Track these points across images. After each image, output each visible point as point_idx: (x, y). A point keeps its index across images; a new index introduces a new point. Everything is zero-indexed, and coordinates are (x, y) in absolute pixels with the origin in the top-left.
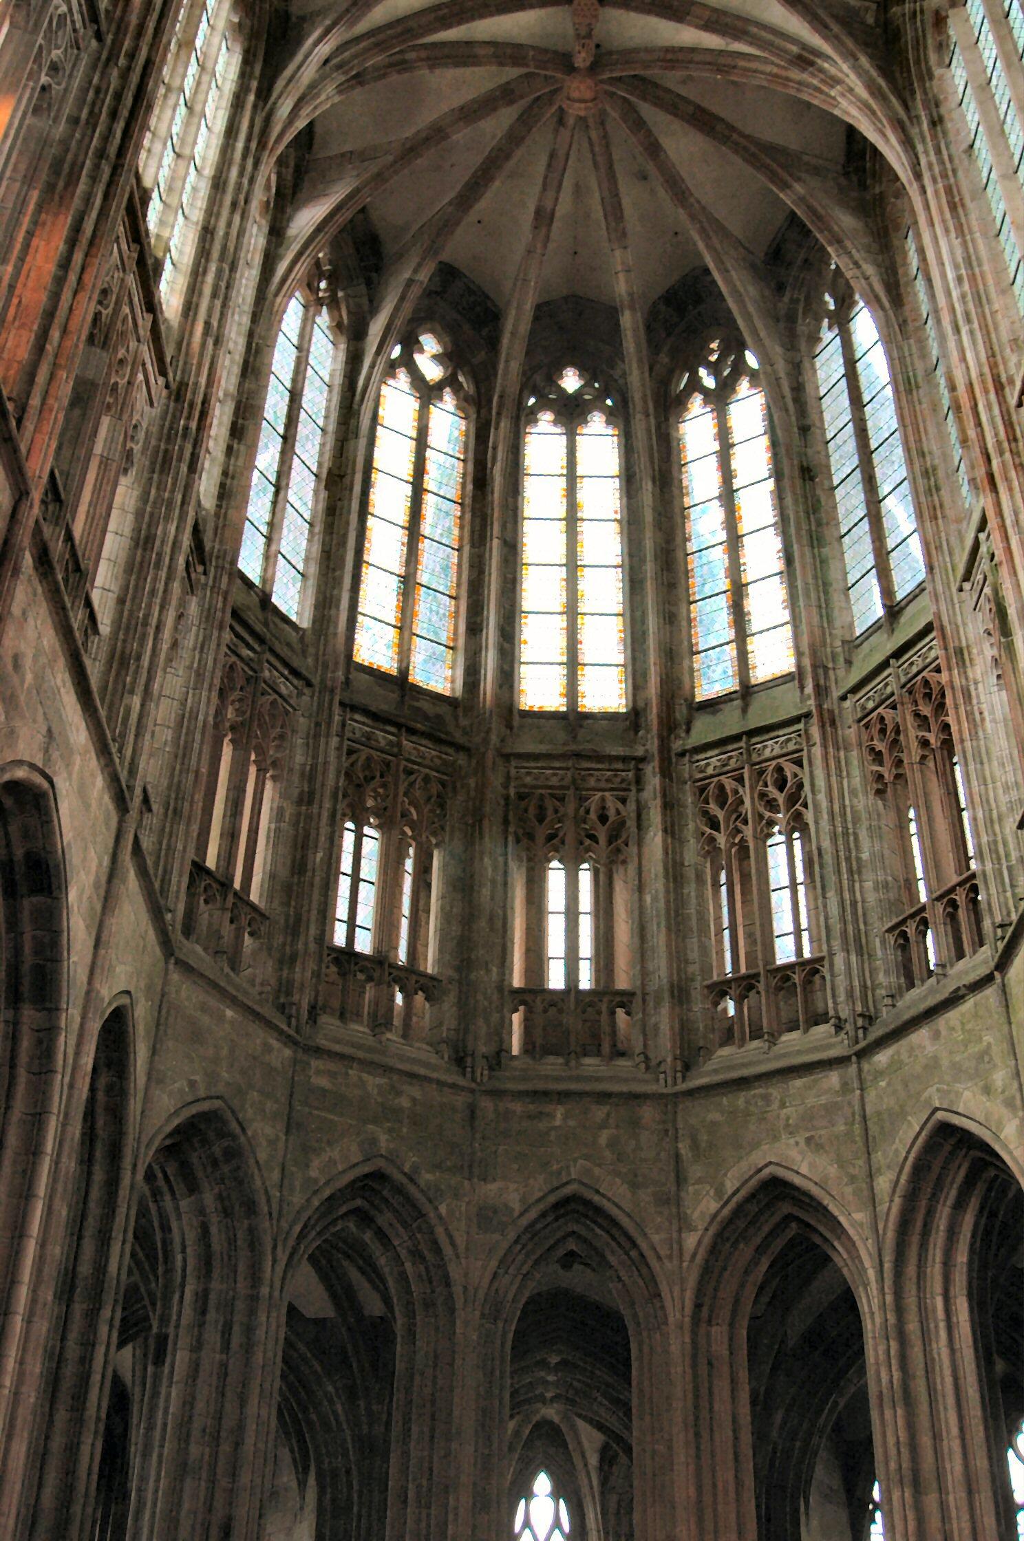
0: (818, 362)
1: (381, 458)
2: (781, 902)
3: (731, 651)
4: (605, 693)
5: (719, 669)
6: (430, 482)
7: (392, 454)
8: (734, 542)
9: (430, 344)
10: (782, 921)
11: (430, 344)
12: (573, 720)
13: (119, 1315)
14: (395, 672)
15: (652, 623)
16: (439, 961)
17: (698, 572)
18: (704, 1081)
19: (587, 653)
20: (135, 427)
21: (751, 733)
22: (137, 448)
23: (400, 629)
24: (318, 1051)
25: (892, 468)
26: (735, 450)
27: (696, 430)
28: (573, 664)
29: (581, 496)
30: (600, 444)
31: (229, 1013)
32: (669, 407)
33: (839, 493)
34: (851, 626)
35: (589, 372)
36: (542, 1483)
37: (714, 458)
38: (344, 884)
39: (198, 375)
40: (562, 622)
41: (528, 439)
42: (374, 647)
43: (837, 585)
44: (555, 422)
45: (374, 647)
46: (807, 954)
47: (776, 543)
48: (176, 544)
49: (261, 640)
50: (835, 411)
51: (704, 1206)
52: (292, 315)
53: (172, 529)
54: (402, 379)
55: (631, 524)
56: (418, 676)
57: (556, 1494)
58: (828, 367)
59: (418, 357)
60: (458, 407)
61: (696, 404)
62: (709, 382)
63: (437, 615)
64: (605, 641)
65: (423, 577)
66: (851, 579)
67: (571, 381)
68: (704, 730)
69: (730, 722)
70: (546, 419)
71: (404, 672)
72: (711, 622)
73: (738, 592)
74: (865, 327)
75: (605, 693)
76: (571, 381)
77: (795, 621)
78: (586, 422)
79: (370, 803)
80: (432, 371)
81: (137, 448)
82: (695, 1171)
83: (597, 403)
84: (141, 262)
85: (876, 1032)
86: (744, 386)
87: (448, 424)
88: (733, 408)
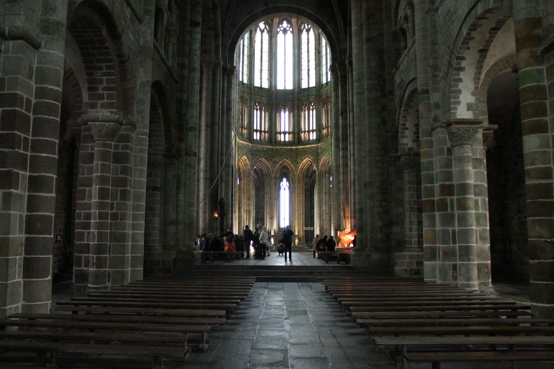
8: (308, 61)
12: (285, 92)
15: (296, 75)
32: (300, 32)
35: (288, 23)
36: (285, 180)
42: (257, 84)
45: (257, 84)
56: (263, 87)
57: (287, 181)
61: (305, 30)
62: (306, 27)
67: (285, 24)
68: (302, 95)
69: (306, 94)
70: (281, 32)
71: (261, 86)
73: (309, 70)
75: (290, 86)
76: (285, 24)
82: (299, 157)
83: (289, 30)
87: (266, 36)
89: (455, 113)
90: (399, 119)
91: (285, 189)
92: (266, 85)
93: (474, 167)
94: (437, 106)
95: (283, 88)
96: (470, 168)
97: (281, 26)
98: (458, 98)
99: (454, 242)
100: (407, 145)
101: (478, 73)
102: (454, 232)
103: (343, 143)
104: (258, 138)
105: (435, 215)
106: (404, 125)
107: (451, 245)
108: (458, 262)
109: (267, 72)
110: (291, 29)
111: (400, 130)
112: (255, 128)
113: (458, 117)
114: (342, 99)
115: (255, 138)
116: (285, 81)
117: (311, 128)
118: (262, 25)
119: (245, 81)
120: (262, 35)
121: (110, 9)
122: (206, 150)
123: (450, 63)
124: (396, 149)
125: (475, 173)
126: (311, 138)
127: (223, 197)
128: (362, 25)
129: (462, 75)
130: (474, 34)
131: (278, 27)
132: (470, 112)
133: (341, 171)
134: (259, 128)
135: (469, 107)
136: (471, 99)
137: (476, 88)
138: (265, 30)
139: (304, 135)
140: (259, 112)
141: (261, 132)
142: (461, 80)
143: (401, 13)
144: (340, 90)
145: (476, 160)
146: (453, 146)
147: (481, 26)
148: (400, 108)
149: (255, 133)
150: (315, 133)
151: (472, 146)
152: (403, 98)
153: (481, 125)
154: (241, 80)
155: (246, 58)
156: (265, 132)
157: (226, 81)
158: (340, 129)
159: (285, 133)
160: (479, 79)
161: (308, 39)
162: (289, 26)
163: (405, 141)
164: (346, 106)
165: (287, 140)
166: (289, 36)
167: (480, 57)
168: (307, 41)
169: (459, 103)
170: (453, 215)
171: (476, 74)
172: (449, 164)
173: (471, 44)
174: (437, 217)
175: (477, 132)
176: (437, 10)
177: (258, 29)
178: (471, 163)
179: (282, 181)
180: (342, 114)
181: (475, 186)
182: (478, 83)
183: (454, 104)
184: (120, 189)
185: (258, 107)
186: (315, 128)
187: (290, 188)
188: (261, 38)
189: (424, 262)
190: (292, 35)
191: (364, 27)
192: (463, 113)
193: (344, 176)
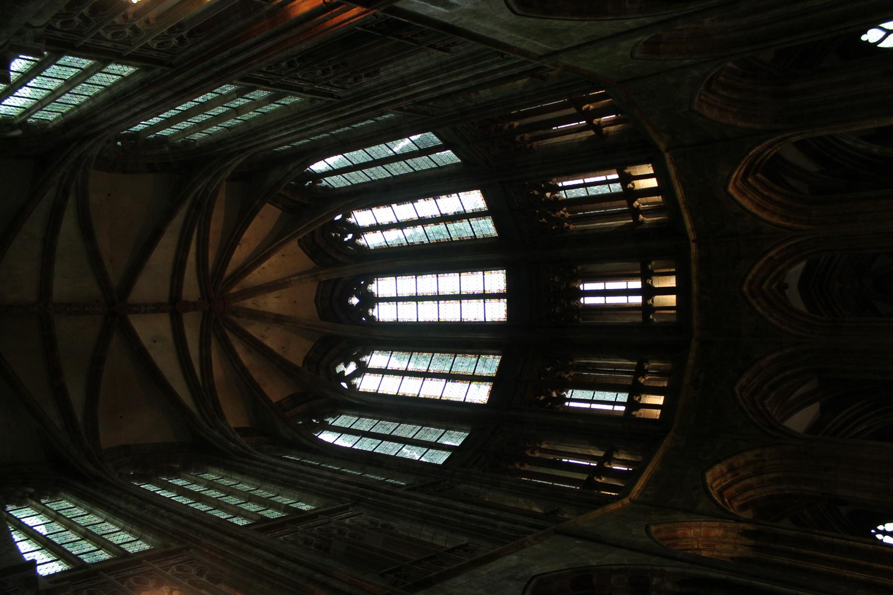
0: (336, 186)
1: (392, 391)
2: (594, 191)
3: (473, 221)
4: (496, 280)
5: (482, 225)
7: (390, 386)
9: (340, 368)
10: (604, 190)
11: (340, 368)
12: (510, 295)
13: (816, 531)
14: (491, 383)
17: (437, 237)
19: (479, 289)
20: (371, 523)
22: (381, 522)
25: (380, 151)
26: (379, 222)
27: (373, 240)
28: (484, 296)
29: (406, 294)
30: (383, 286)
33: (395, 174)
34: (457, 164)
37: (384, 233)
38: (594, 406)
39: (348, 489)
40: (464, 302)
41: (381, 320)
44: (373, 308)
45: (480, 394)
46: (616, 176)
47: (421, 201)
48: (425, 501)
50: (358, 177)
52: (327, 437)
53: (419, 503)
54: (357, 381)
55: (417, 270)
58: (337, 182)
59: (347, 373)
60: (368, 355)
61: (361, 242)
63: (464, 364)
64: (472, 281)
65: (447, 369)
66: (434, 166)
67: (355, 301)
72: (461, 230)
74: (319, 167)
75: (496, 280)
76: (355, 301)
77: (457, 191)
78: (372, 293)
79: (554, 395)
80: (352, 367)
81: (381, 522)
84: (293, 522)
86: (352, 220)
87: (377, 360)
88: (361, 224)
92: (490, 365)
104: (659, 400)
117: (617, 188)
119: (455, 439)
126: (652, 183)
134: (623, 397)
139: (646, 212)
141: (636, 390)
149: (644, 413)
159: (648, 292)
165: (671, 282)
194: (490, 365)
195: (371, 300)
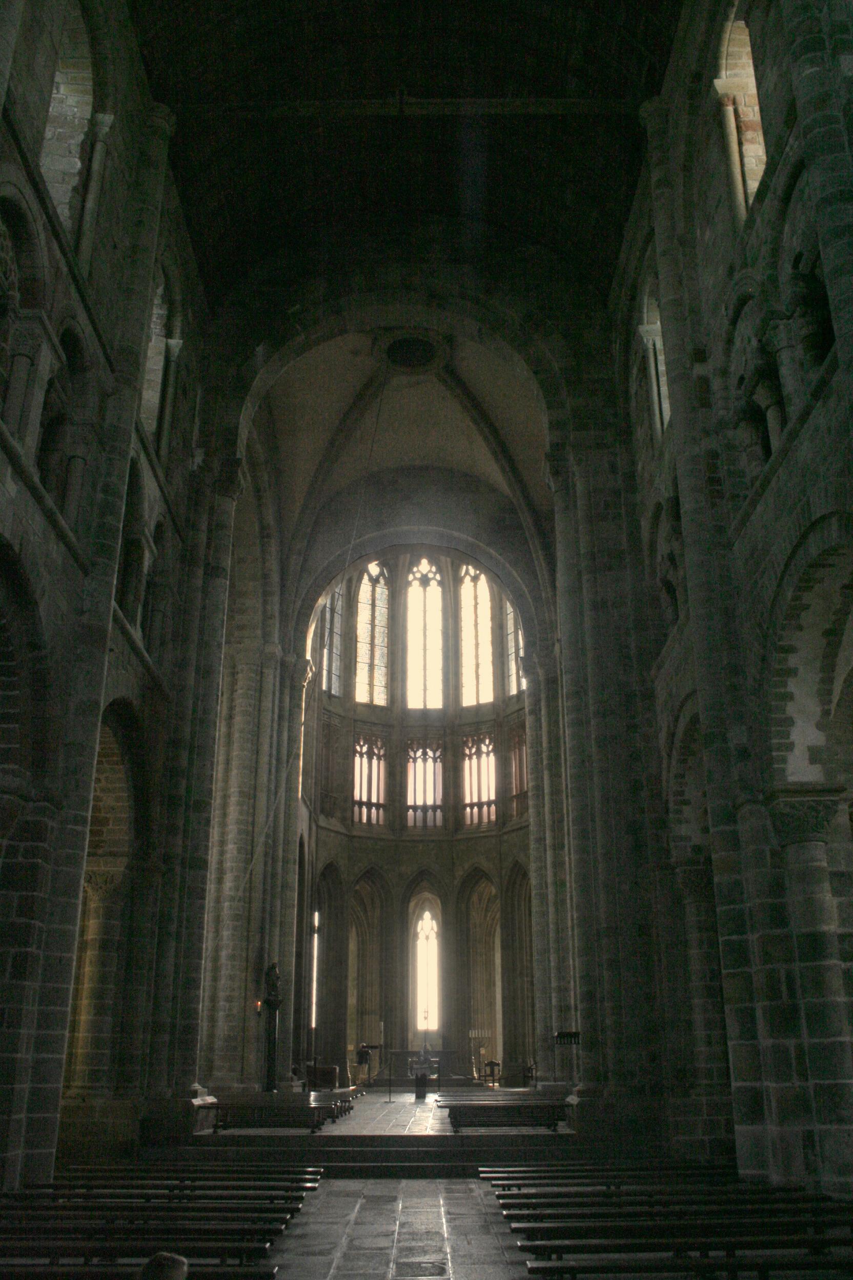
6: (377, 622)
12: (425, 713)
16: (385, 799)
18: (459, 837)
21: (478, 723)
23: (369, 689)
24: (354, 837)
31: (332, 834)
32: (458, 581)
34: (509, 691)
36: (427, 915)
43: (506, 675)
45: (361, 696)
49: (329, 711)
51: (460, 873)
60: (385, 584)
67: (424, 566)
70: (416, 584)
71: (372, 700)
75: (436, 702)
76: (424, 566)
83: (434, 578)
85: (504, 830)
87: (382, 591)
89: (784, 770)
90: (668, 782)
91: (427, 938)
92: (380, 699)
93: (836, 893)
94: (744, 754)
95: (421, 707)
96: (828, 899)
97: (415, 569)
98: (788, 735)
99: (804, 1076)
100: (689, 839)
101: (828, 681)
102: (800, 1048)
103: (553, 831)
105: (753, 1009)
106: (682, 793)
107: (798, 1084)
108: (818, 1127)
109: (384, 669)
110: (438, 577)
111: (671, 805)
112: (357, 797)
113: (791, 779)
114: (549, 733)
115: (356, 819)
116: (425, 690)
118: (374, 568)
120: (373, 591)
121: (17, 548)
122: (239, 850)
123: (763, 659)
124: (668, 852)
125: (840, 906)
127: (276, 960)
128: (580, 573)
129: (792, 686)
130: (807, 598)
131: (410, 571)
132: (817, 768)
133: (551, 897)
134: (365, 799)
135: (815, 755)
136: (817, 738)
137: (826, 713)
138: (382, 581)
140: (365, 759)
142: (790, 697)
143: (663, 549)
144: (543, 712)
145: (837, 876)
146: (783, 847)
147: (821, 581)
148: (669, 756)
150: (493, 808)
151: (827, 843)
152: (673, 735)
153: (843, 795)
154: (324, 687)
155: (337, 640)
156: (378, 806)
157: (287, 691)
158: (547, 798)
160: (830, 692)
161: (476, 598)
162: (434, 569)
163: (684, 830)
164: (558, 747)
166: (435, 591)
167: (829, 644)
168: (473, 603)
169: (790, 747)
170: (795, 1009)
171: (823, 681)
172: (777, 887)
173: (806, 618)
174: (759, 1013)
175: (836, 812)
176: (729, 546)
177: (366, 577)
178: (827, 886)
179: (420, 917)
180: (550, 767)
181: (842, 938)
182: (830, 702)
183: (778, 750)
184: (13, 951)
185: (365, 749)
186: (493, 797)
187: (438, 934)
188: (370, 596)
189: (736, 1127)
190: (439, 589)
191: (585, 578)
192: (800, 769)
193: (557, 910)
194: (380, 699)
195: (425, 581)
